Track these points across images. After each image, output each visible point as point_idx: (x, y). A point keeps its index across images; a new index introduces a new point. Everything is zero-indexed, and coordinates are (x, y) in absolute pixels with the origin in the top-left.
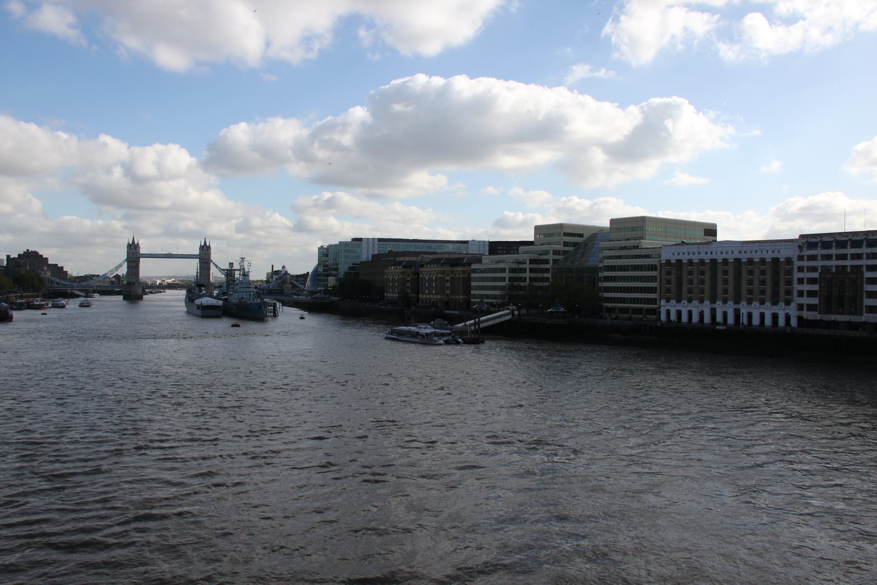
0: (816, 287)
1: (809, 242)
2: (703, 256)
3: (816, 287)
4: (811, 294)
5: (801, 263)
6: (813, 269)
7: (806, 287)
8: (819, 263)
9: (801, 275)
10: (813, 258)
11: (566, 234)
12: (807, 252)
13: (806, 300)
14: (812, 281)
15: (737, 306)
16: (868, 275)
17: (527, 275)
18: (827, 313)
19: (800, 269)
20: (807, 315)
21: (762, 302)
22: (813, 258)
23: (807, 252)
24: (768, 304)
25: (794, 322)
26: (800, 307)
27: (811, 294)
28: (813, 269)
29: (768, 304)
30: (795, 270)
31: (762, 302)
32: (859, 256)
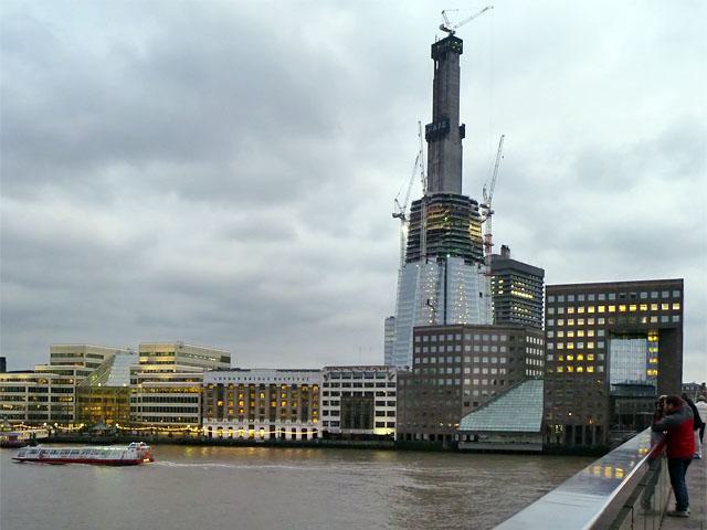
0: (338, 408)
1: (332, 372)
2: (242, 381)
3: (338, 408)
4: (335, 413)
5: (326, 389)
6: (334, 394)
7: (330, 408)
8: (341, 389)
9: (325, 398)
10: (337, 385)
11: (90, 356)
12: (331, 381)
13: (330, 418)
14: (336, 403)
15: (272, 423)
16: (377, 399)
17: (49, 395)
18: (350, 427)
19: (326, 394)
20: (330, 429)
21: (294, 419)
22: (337, 385)
23: (331, 381)
24: (299, 421)
25: (320, 435)
26: (325, 423)
27: (335, 413)
28: (334, 394)
29: (299, 421)
30: (321, 394)
31: (294, 419)
32: (371, 385)
